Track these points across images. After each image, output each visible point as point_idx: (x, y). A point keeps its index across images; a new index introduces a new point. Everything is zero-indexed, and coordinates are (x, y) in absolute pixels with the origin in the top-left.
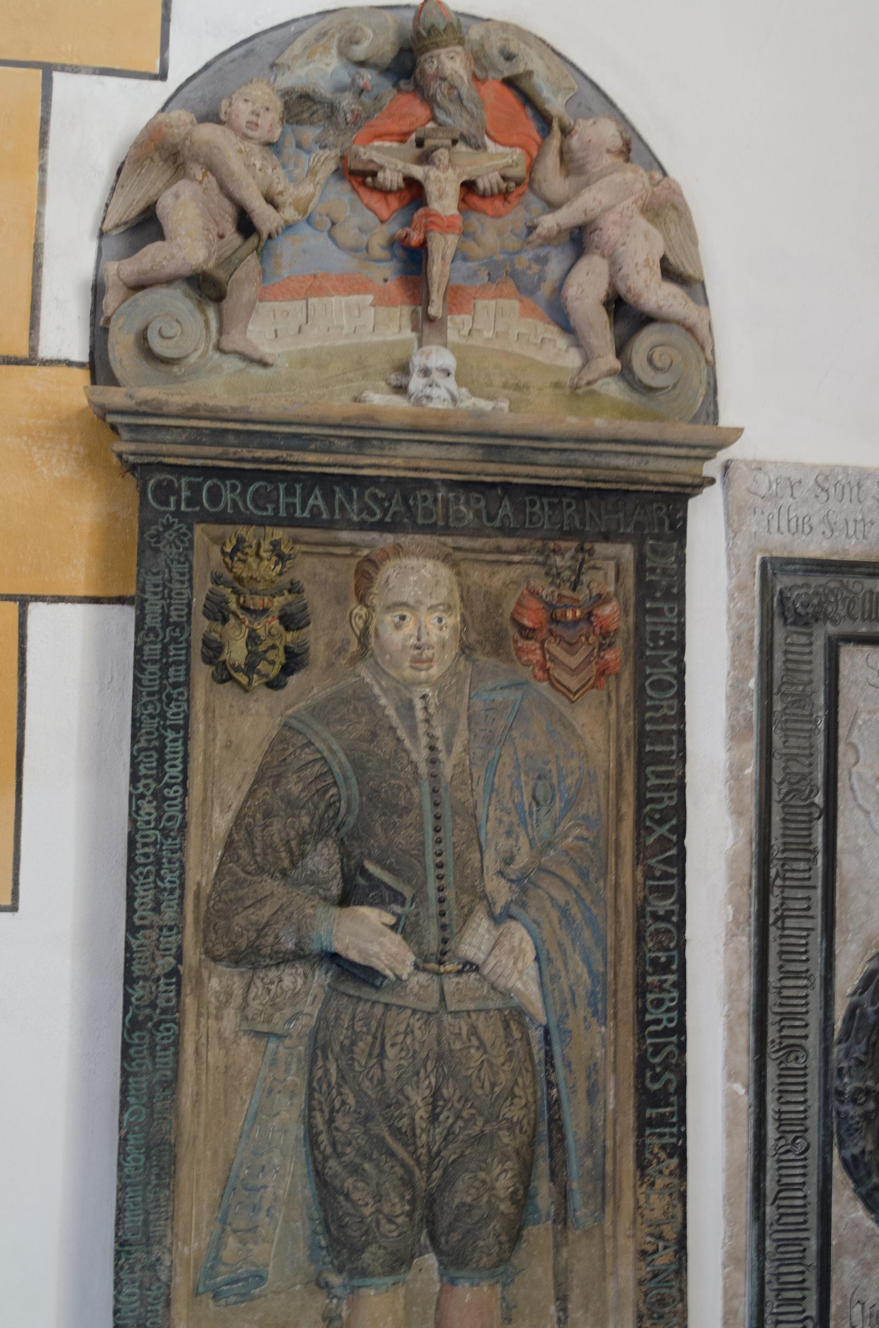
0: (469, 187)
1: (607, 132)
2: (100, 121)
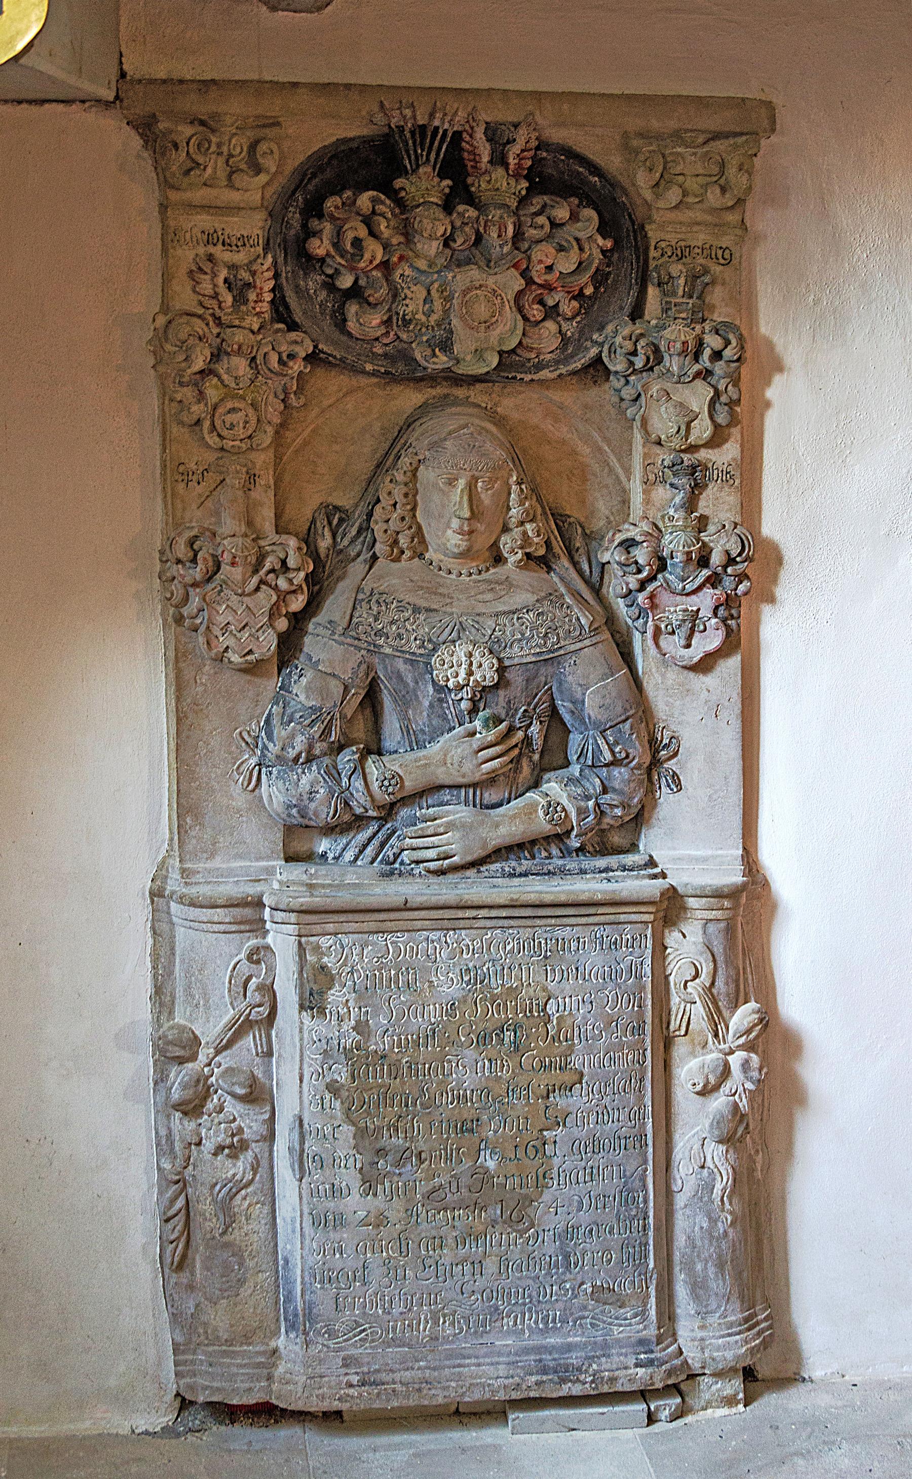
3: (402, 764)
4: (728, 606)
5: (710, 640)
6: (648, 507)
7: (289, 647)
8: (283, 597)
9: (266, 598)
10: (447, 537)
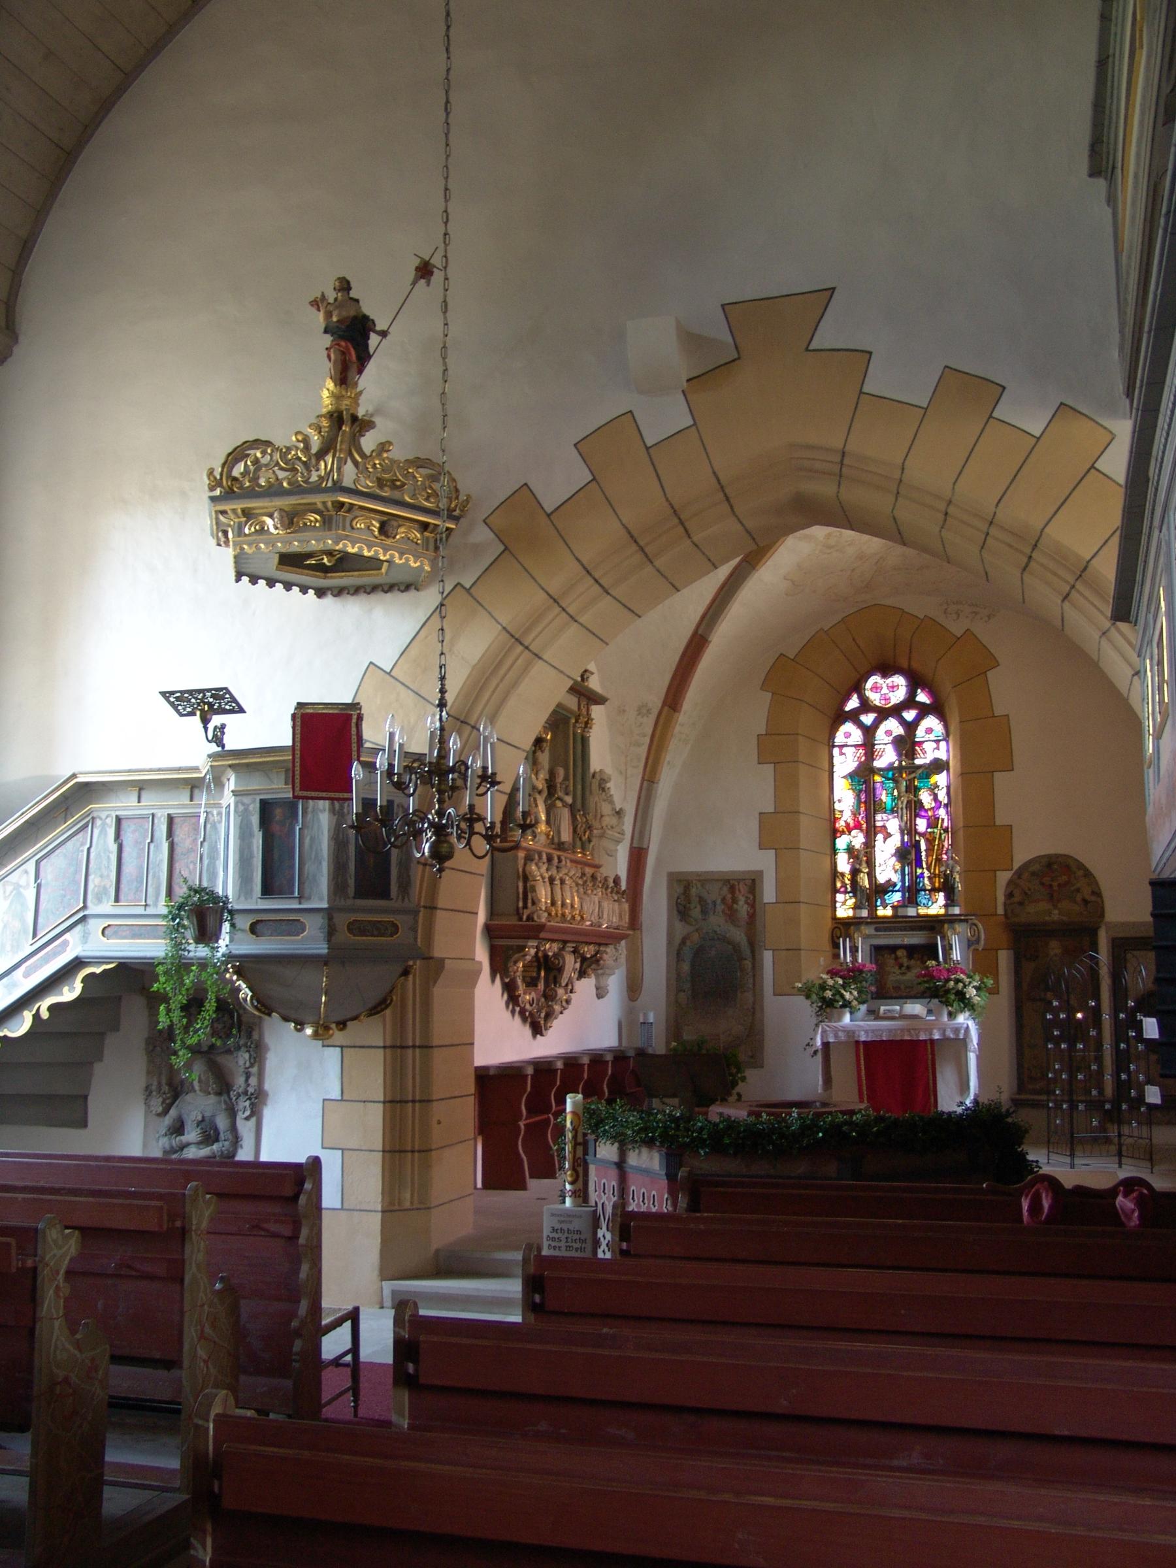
0: (1059, 885)
1: (1081, 873)
2: (1004, 877)
3: (184, 1139)
4: (252, 1105)
5: (248, 1113)
6: (240, 1081)
7: (166, 1112)
8: (164, 1100)
9: (161, 1100)
10: (197, 1087)
